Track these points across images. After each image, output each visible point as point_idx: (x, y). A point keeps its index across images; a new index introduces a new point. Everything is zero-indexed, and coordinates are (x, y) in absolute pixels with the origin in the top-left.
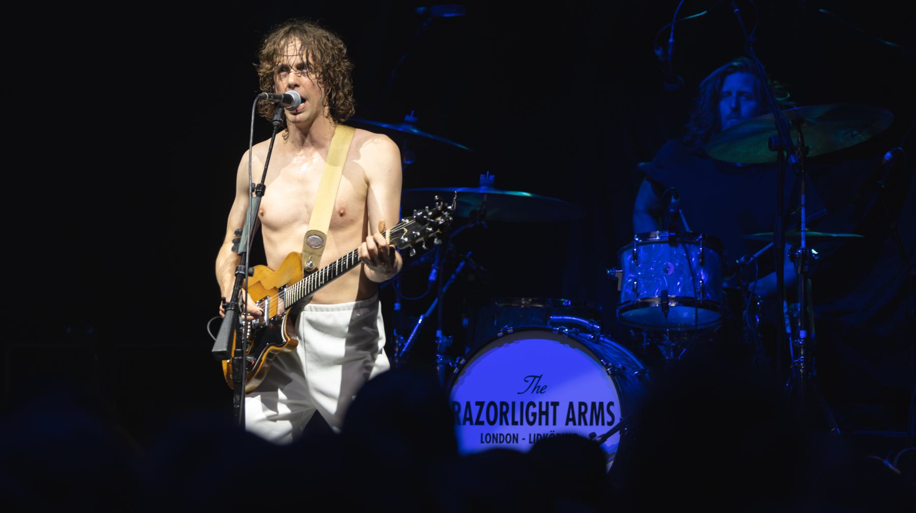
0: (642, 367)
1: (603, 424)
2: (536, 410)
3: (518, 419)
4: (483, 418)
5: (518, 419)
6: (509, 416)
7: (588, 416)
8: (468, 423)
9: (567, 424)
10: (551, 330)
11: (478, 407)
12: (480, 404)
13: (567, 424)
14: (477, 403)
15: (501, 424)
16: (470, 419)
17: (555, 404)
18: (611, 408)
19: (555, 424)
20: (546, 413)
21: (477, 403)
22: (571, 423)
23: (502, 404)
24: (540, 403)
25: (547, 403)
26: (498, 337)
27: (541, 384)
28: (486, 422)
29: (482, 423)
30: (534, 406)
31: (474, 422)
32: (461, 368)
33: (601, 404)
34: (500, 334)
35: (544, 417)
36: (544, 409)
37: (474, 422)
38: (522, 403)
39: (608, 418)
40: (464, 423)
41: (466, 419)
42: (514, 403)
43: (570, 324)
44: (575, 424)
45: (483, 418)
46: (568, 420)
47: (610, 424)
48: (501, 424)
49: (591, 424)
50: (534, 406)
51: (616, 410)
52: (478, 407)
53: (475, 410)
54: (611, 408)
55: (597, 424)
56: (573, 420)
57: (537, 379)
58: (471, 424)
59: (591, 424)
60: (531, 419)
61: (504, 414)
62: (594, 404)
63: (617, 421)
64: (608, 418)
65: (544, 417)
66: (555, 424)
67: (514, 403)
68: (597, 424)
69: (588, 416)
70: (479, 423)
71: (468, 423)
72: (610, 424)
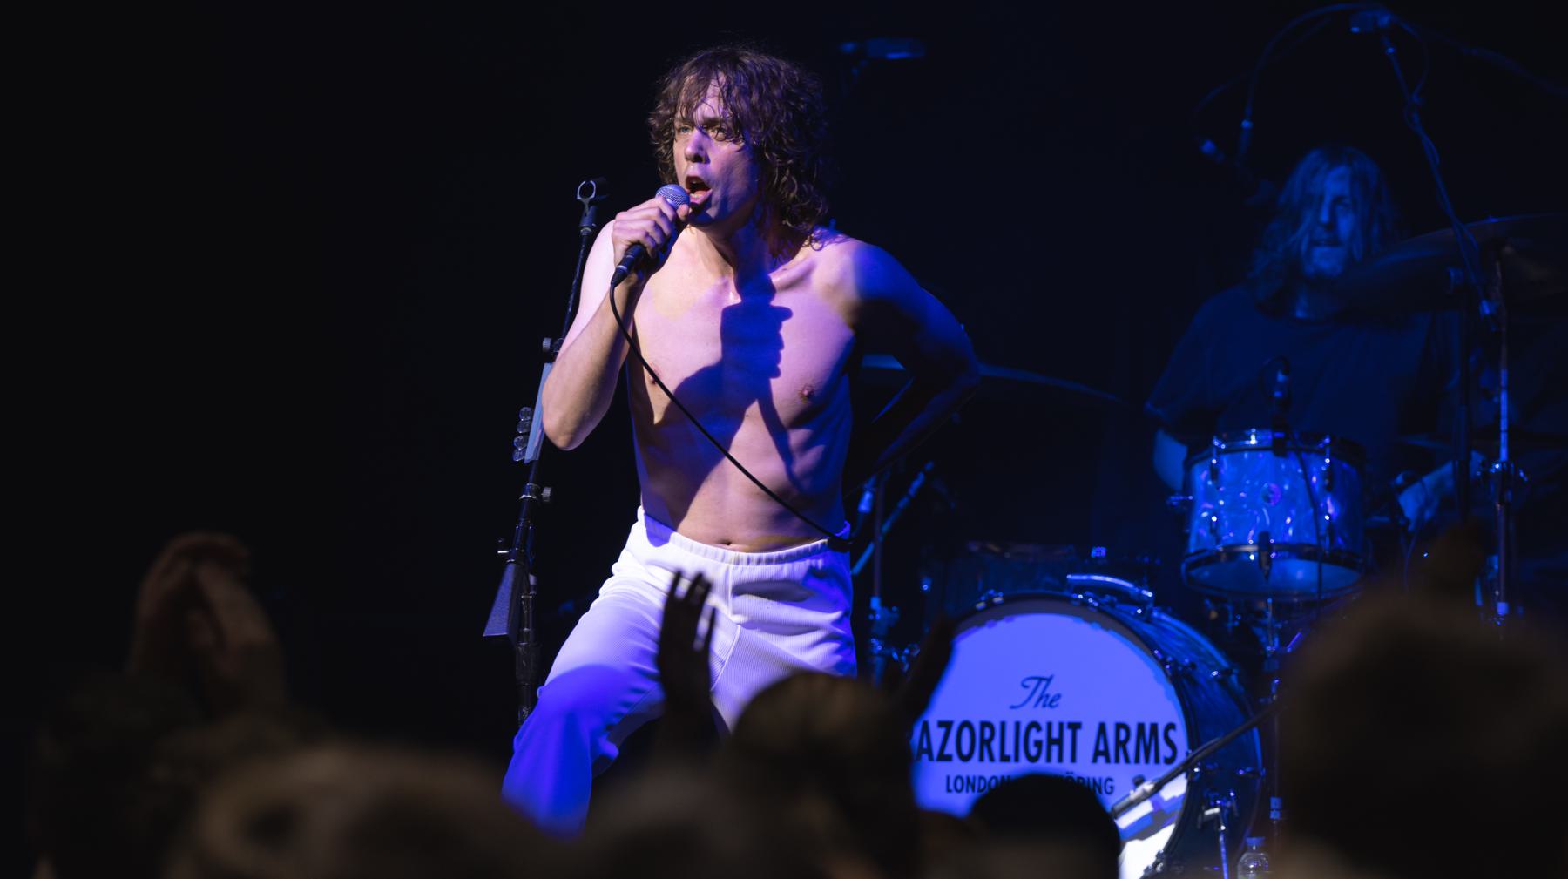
0: (1224, 664)
2: (1042, 736)
3: (1010, 750)
4: (951, 749)
5: (1010, 750)
6: (996, 745)
7: (1131, 747)
9: (1095, 760)
10: (1068, 600)
11: (942, 731)
12: (946, 725)
13: (1095, 760)
15: (981, 759)
17: (1075, 727)
18: (1172, 734)
19: (1073, 760)
20: (1059, 742)
21: (941, 724)
22: (1101, 759)
23: (984, 725)
24: (1049, 725)
25: (1061, 725)
26: (976, 611)
27: (1052, 691)
28: (956, 758)
29: (949, 758)
30: (1039, 729)
31: (935, 754)
33: (1154, 727)
34: (981, 605)
35: (1055, 749)
36: (1055, 735)
37: (935, 754)
38: (1018, 725)
39: (1165, 751)
42: (1003, 725)
44: (1108, 761)
45: (951, 749)
46: (1097, 753)
47: (1169, 761)
48: (981, 759)
49: (1137, 761)
50: (1039, 729)
51: (1180, 737)
52: (942, 731)
53: (937, 735)
54: (1172, 734)
55: (1147, 761)
56: (1106, 753)
59: (1137, 761)
60: (1033, 751)
61: (986, 743)
62: (1141, 727)
63: (1181, 758)
64: (1165, 751)
65: (1055, 749)
66: (1073, 760)
67: (1003, 725)
68: (1147, 761)
69: (1131, 747)
70: (944, 757)
72: (1169, 761)
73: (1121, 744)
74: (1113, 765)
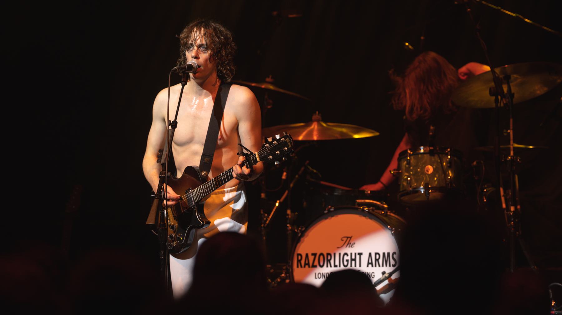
1: (390, 266)
2: (349, 258)
3: (337, 263)
5: (337, 263)
6: (332, 262)
7: (381, 261)
8: (307, 266)
9: (368, 266)
10: (357, 209)
11: (313, 257)
12: (314, 255)
13: (368, 266)
14: (313, 254)
15: (327, 266)
16: (308, 264)
17: (360, 254)
19: (360, 266)
20: (355, 260)
21: (313, 254)
22: (370, 266)
24: (351, 254)
25: (355, 254)
31: (311, 264)
32: (303, 233)
34: (326, 212)
35: (353, 262)
36: (353, 257)
37: (311, 264)
39: (392, 262)
40: (305, 267)
41: (305, 264)
43: (369, 205)
44: (372, 266)
45: (316, 263)
46: (368, 264)
47: (393, 266)
48: (327, 266)
49: (383, 266)
52: (313, 257)
53: (311, 258)
54: (395, 256)
55: (386, 266)
56: (372, 263)
57: (349, 239)
58: (309, 267)
59: (383, 266)
60: (346, 263)
62: (384, 254)
65: (353, 262)
66: (360, 266)
68: (386, 266)
69: (381, 261)
71: (307, 266)
72: (393, 266)
73: (377, 260)
74: (374, 267)
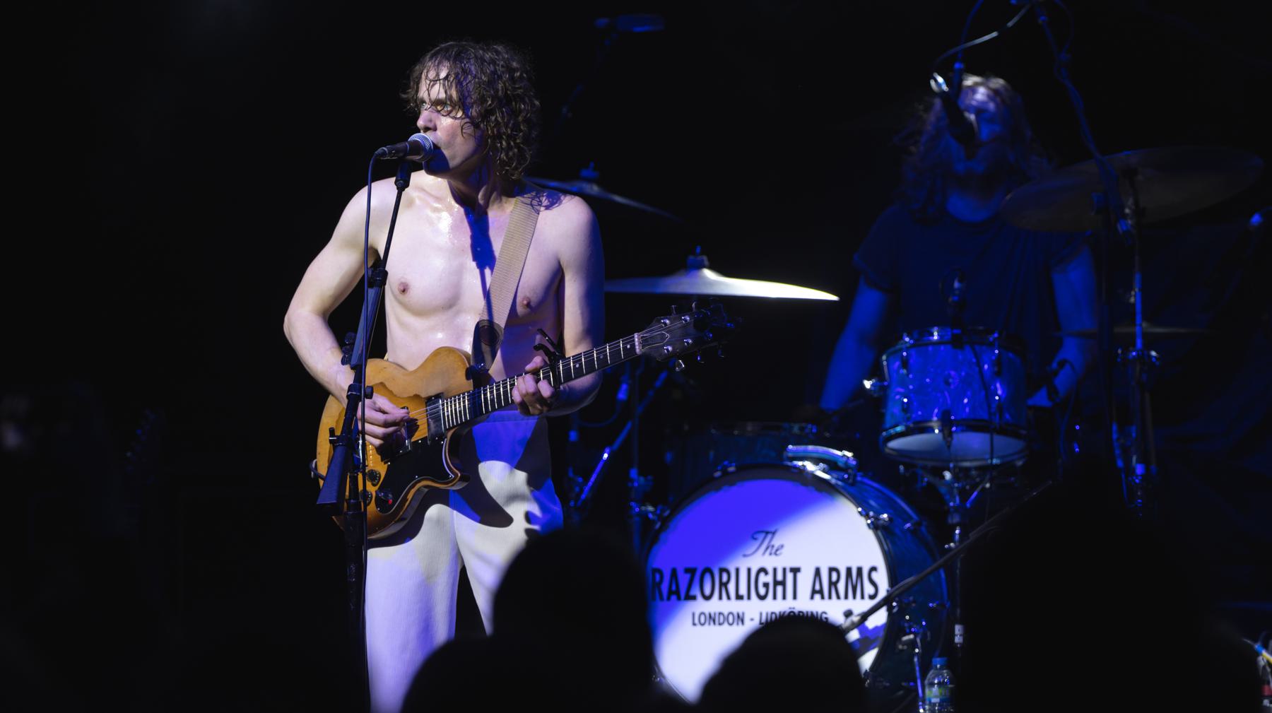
1: (863, 597)
2: (769, 579)
3: (743, 591)
5: (743, 591)
9: (812, 598)
11: (688, 576)
13: (812, 598)
14: (687, 571)
15: (720, 598)
17: (795, 571)
18: (874, 575)
19: (795, 597)
20: (783, 583)
21: (687, 571)
22: (817, 596)
24: (775, 570)
25: (784, 570)
30: (766, 573)
32: (665, 522)
34: (718, 474)
35: (780, 589)
36: (780, 577)
39: (869, 589)
40: (669, 599)
41: (670, 592)
44: (823, 598)
46: (814, 592)
47: (872, 597)
48: (720, 598)
49: (846, 597)
50: (766, 573)
51: (882, 578)
54: (874, 575)
55: (854, 597)
56: (821, 592)
59: (846, 597)
60: (762, 591)
62: (849, 570)
63: (882, 594)
64: (869, 589)
65: (780, 589)
66: (795, 597)
68: (854, 597)
72: (872, 597)
73: (833, 584)
74: (826, 601)
